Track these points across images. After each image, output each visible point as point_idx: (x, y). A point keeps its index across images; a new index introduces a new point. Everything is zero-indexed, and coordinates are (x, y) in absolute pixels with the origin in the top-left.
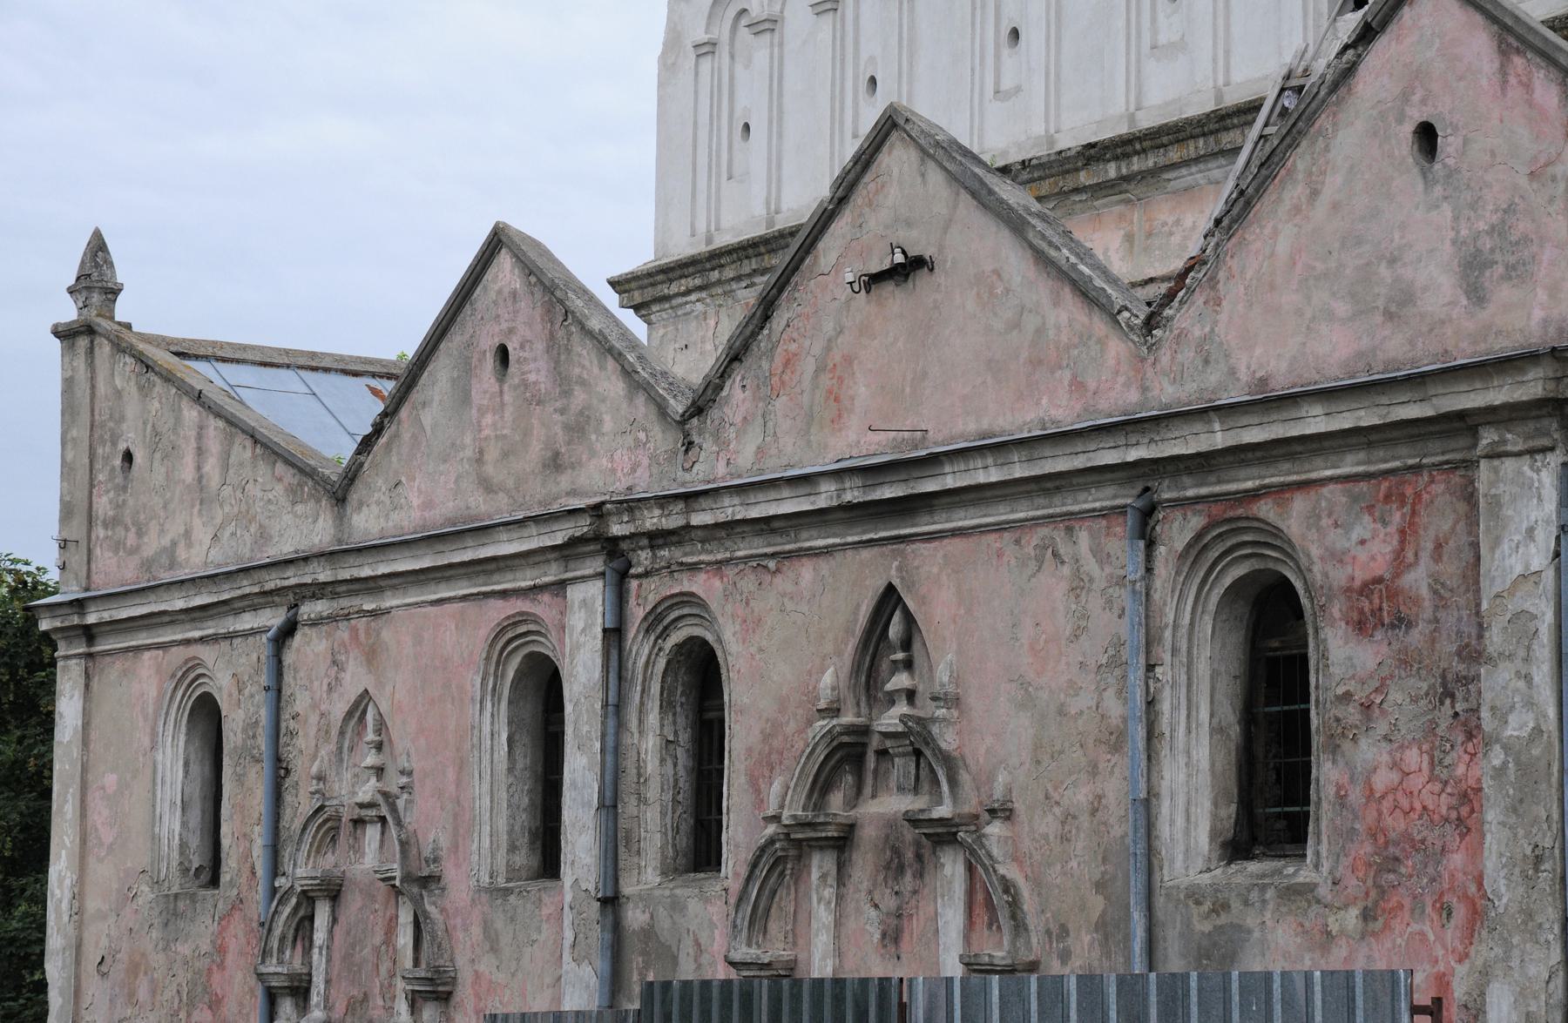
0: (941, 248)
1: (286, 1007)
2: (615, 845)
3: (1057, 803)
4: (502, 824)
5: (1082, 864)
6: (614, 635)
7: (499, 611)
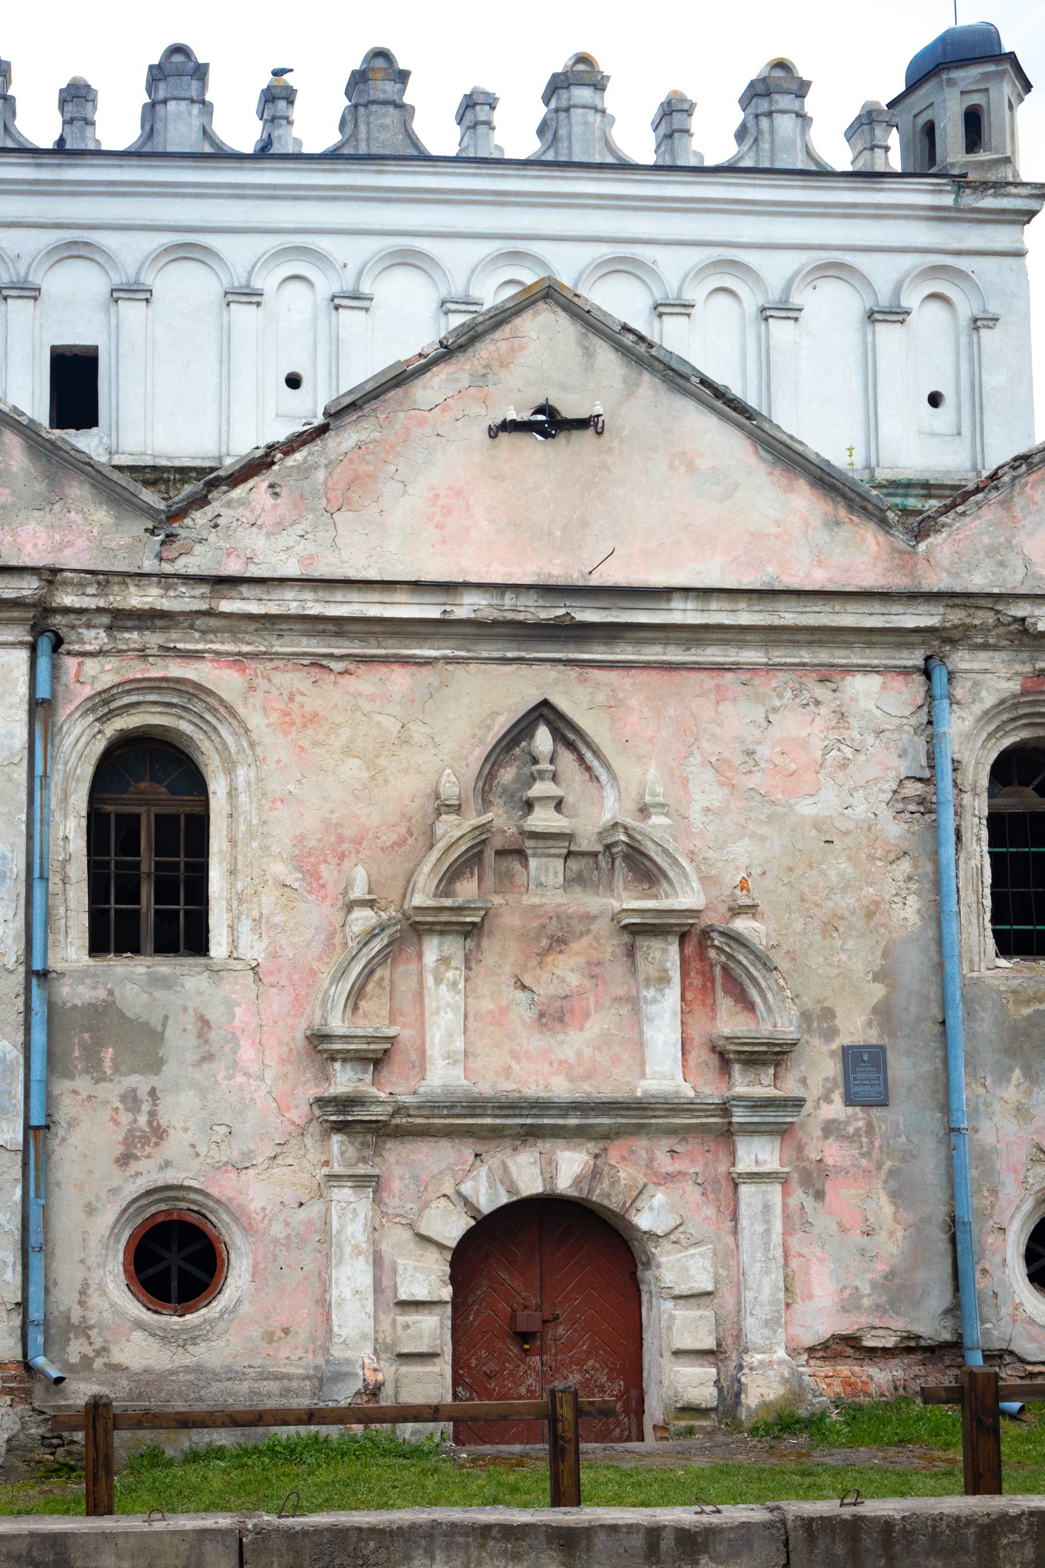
3: (817, 905)
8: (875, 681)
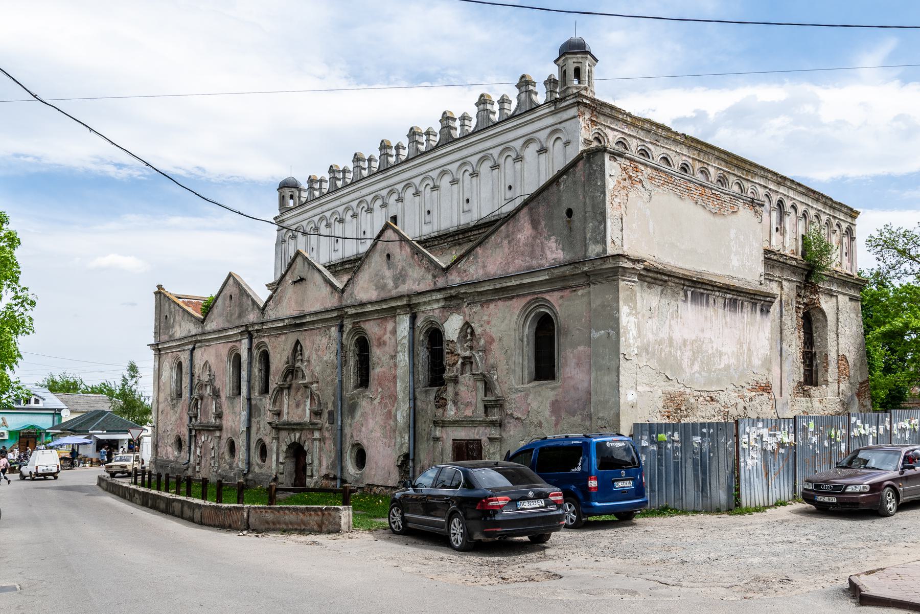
0: (307, 276)
1: (193, 420)
2: (250, 389)
4: (231, 385)
5: (330, 391)
6: (250, 349)
7: (231, 345)
8: (334, 328)
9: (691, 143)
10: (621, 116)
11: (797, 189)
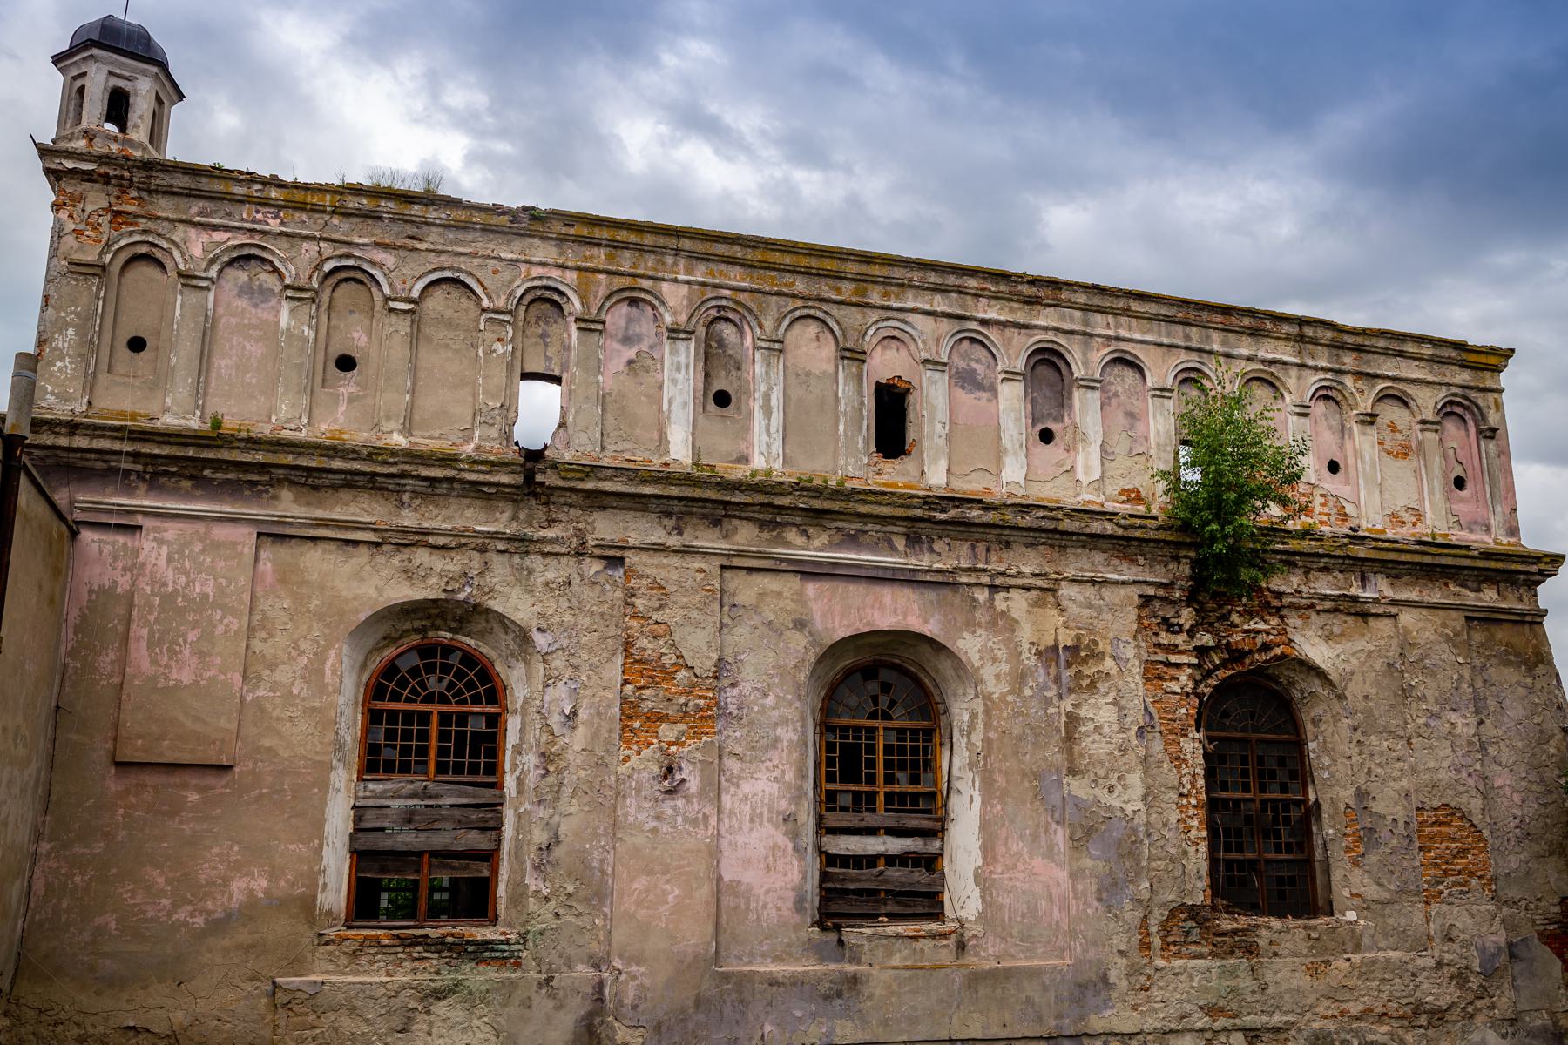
9: (564, 230)
10: (239, 190)
11: (1129, 310)
